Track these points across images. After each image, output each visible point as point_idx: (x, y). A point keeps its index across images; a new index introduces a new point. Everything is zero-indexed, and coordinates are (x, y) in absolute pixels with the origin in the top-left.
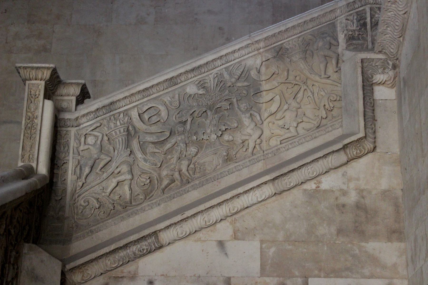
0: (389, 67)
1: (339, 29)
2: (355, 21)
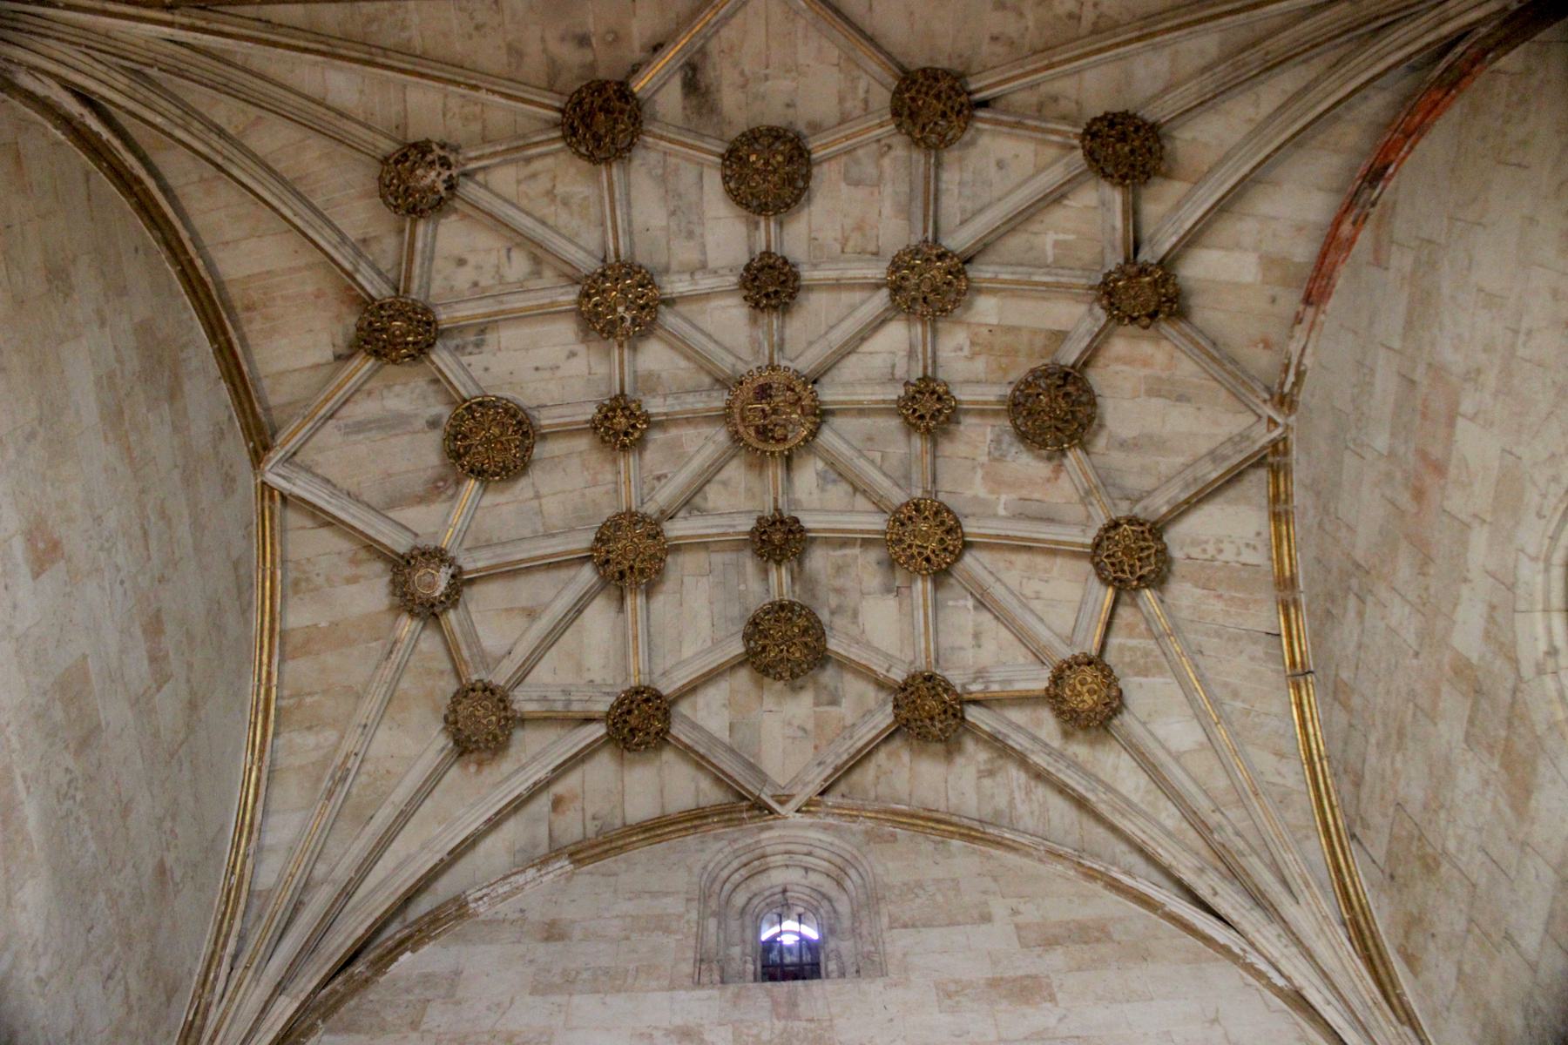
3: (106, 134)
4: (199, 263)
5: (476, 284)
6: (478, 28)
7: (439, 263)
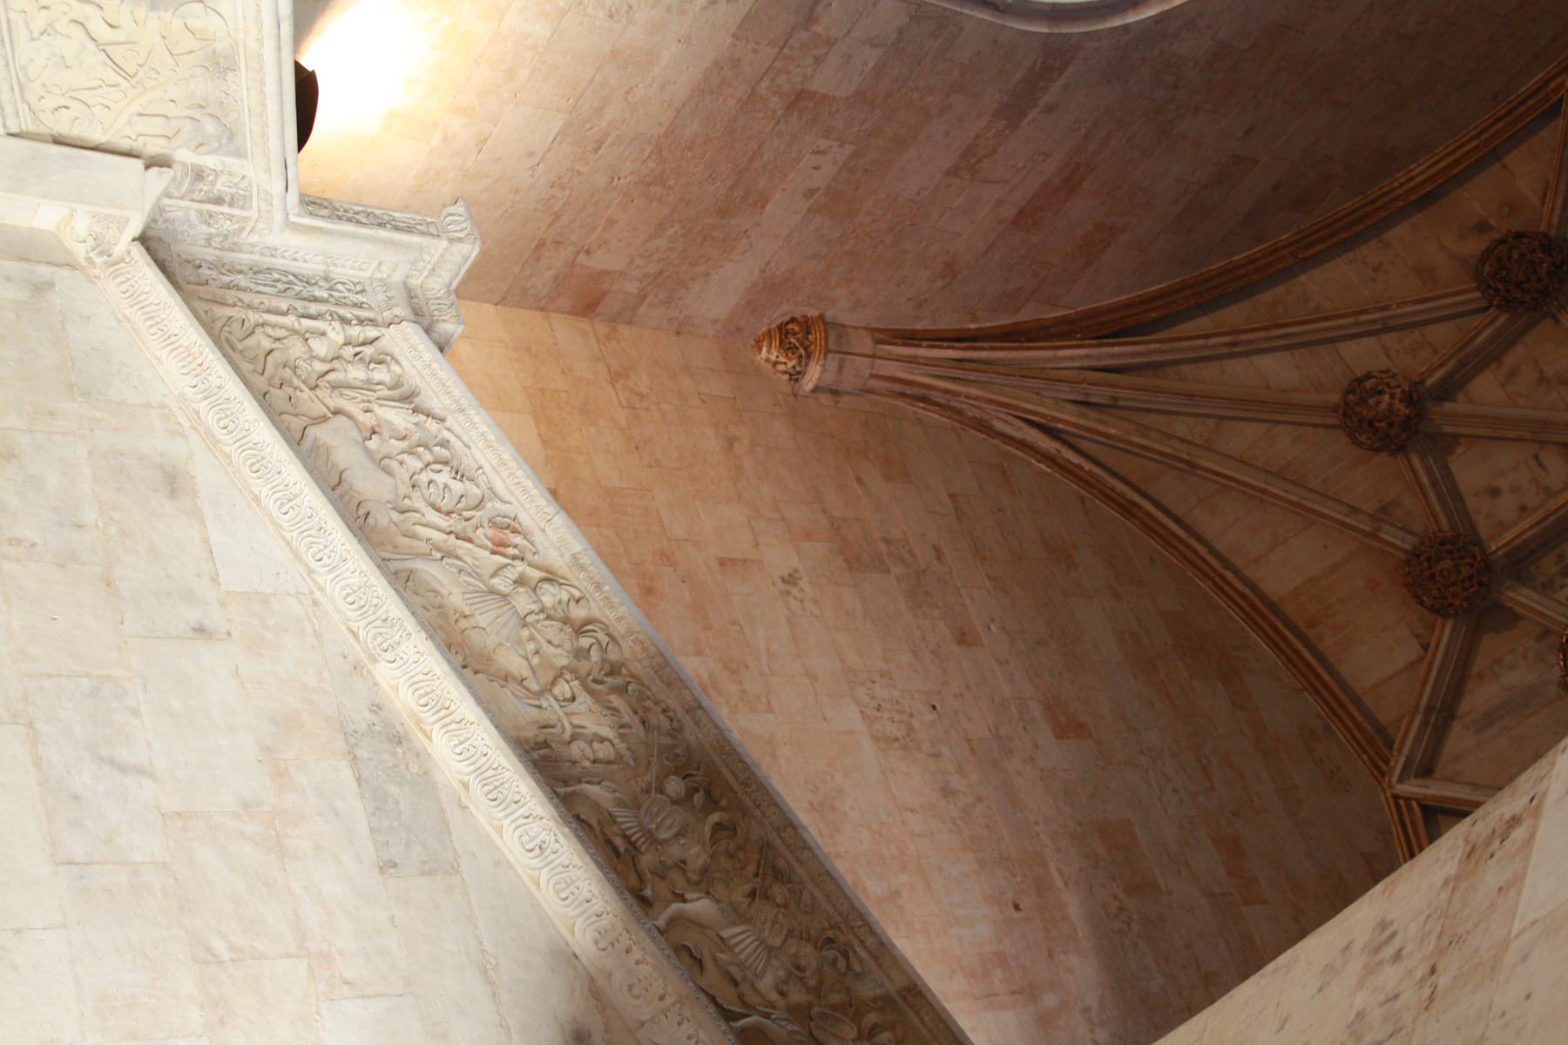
0: (95, 252)
1: (230, 160)
2: (234, 190)
3: (1087, 466)
4: (1229, 575)
5: (1523, 509)
6: (1375, 270)
7: (1471, 503)
